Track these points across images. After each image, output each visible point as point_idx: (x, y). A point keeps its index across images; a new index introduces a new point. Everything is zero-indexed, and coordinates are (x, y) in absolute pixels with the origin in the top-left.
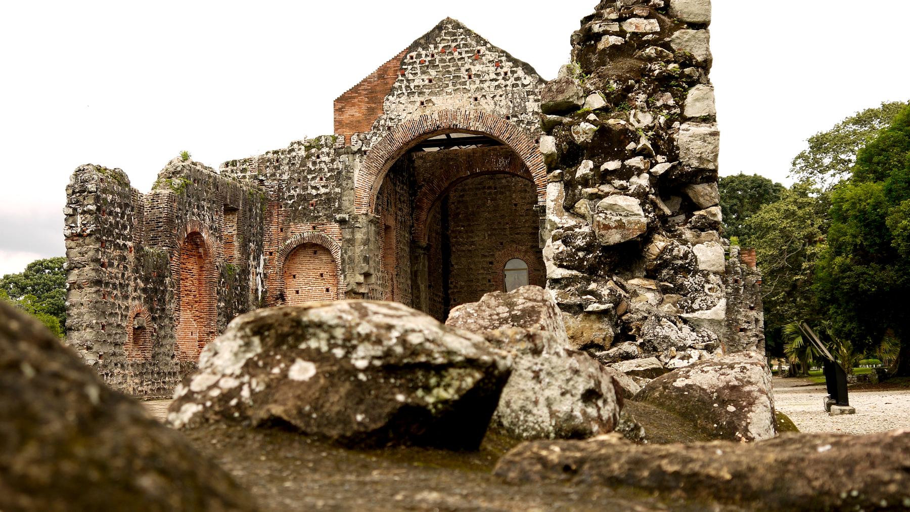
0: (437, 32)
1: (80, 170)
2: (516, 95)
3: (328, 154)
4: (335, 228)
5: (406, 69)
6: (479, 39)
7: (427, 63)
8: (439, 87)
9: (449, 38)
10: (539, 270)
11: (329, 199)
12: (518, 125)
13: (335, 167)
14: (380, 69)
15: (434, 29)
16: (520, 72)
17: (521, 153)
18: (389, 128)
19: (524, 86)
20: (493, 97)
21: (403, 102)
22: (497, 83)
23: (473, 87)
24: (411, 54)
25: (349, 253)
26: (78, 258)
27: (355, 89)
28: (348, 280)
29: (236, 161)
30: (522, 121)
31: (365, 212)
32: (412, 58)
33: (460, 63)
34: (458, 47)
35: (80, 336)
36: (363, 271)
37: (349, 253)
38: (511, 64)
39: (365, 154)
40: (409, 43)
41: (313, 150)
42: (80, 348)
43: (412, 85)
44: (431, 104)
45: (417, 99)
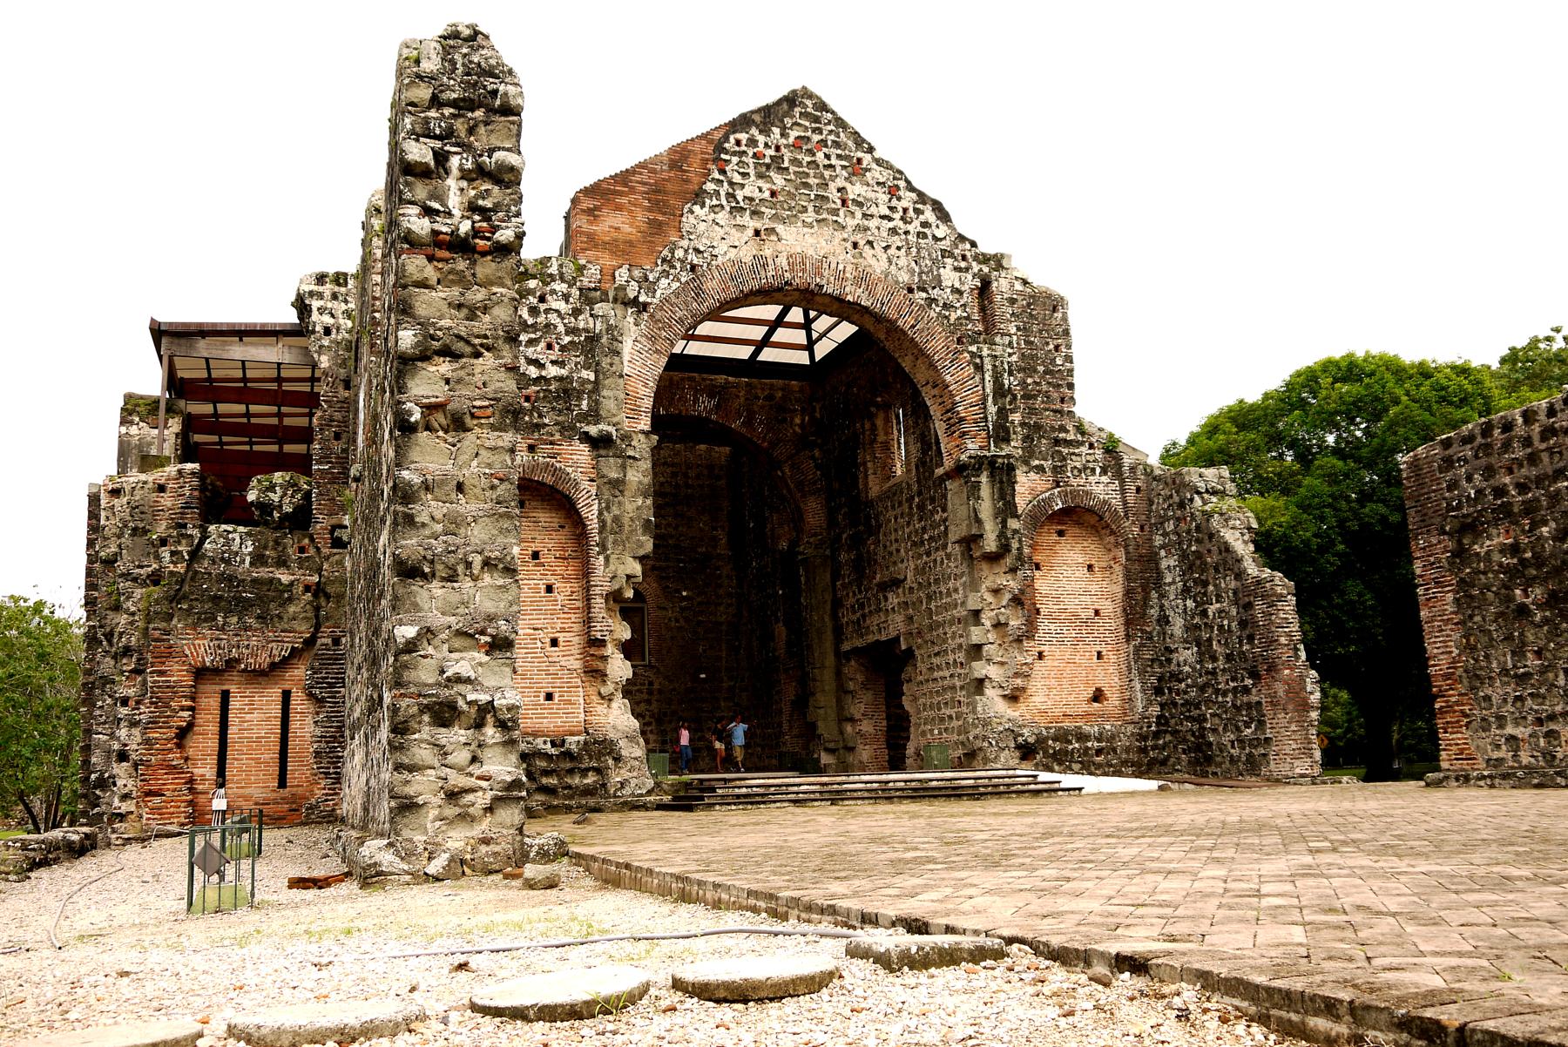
0: (785, 106)
1: (455, 35)
2: (924, 253)
3: (566, 297)
6: (859, 141)
7: (767, 160)
9: (807, 124)
10: (664, 609)
11: (566, 392)
12: (930, 306)
13: (582, 325)
14: (672, 150)
15: (779, 103)
16: (929, 215)
17: (936, 358)
18: (693, 268)
19: (936, 239)
20: (887, 248)
21: (722, 223)
22: (891, 225)
24: (739, 136)
25: (615, 511)
27: (623, 178)
28: (612, 567)
29: (345, 275)
31: (647, 428)
32: (738, 143)
33: (827, 174)
34: (823, 143)
35: (454, 598)
36: (641, 552)
37: (615, 511)
38: (914, 196)
39: (645, 310)
40: (733, 114)
41: (532, 284)
42: (458, 642)
43: (740, 195)
44: (774, 238)
45: (752, 224)
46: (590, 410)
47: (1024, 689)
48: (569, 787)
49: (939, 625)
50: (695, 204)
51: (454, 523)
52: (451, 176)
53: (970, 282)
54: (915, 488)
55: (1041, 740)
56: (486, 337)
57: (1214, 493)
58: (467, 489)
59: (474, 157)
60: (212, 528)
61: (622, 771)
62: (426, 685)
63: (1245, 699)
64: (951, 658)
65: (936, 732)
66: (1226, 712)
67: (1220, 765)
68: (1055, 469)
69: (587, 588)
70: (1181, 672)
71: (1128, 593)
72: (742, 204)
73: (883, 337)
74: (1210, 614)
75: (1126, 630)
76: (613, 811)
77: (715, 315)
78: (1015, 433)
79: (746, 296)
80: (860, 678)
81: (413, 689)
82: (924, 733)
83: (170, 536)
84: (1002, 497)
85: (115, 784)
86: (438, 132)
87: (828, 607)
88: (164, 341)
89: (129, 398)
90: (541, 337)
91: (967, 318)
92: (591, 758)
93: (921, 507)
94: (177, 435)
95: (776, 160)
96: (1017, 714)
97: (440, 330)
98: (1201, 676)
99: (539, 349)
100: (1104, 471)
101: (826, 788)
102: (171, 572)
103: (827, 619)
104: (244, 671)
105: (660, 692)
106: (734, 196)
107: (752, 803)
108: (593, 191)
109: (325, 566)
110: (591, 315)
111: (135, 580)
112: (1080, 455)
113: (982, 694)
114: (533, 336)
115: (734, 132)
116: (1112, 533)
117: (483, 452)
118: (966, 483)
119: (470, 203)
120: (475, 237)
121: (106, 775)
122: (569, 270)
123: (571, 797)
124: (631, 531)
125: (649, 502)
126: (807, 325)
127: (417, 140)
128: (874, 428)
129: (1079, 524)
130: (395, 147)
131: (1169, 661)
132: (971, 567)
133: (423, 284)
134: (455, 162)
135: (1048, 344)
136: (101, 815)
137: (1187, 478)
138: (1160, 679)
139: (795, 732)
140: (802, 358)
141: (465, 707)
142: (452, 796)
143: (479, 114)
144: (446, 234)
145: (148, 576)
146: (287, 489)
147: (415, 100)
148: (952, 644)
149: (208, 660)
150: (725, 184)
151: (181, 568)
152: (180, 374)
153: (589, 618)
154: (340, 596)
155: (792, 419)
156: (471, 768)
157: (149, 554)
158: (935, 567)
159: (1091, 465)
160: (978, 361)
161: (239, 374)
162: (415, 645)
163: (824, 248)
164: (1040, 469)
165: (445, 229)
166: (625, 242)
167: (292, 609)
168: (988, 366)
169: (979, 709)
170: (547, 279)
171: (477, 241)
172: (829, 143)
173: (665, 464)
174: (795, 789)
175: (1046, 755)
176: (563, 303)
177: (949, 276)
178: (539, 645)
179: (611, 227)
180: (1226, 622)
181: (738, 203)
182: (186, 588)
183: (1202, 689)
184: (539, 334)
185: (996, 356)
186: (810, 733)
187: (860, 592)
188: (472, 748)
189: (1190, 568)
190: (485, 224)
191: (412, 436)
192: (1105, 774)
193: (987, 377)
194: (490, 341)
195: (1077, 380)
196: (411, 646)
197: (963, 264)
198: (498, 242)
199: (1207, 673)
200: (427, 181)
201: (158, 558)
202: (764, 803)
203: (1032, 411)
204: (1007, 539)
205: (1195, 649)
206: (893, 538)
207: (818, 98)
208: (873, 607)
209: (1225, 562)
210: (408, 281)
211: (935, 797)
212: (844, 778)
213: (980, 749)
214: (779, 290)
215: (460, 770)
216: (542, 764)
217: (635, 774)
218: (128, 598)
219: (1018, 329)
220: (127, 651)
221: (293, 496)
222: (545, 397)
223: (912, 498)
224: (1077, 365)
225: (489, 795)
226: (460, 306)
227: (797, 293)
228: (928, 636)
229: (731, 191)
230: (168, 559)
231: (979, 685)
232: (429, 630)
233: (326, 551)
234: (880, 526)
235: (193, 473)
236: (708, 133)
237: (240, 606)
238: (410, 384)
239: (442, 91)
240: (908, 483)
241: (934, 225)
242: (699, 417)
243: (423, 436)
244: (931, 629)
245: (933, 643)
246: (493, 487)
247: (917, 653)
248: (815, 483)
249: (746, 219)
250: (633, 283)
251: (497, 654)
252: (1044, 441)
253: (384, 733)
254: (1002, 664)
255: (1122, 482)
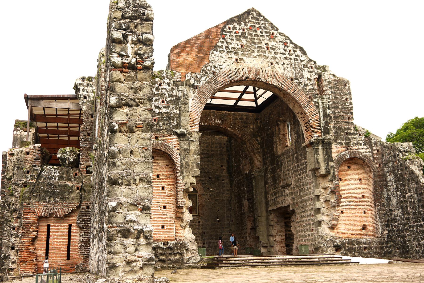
0: (246, 15)
2: (297, 66)
3: (169, 84)
4: (174, 139)
5: (226, 35)
6: (273, 26)
7: (240, 34)
8: (248, 51)
9: (254, 21)
10: (204, 195)
11: (169, 118)
12: (299, 85)
13: (174, 94)
14: (206, 31)
15: (244, 14)
16: (299, 52)
18: (214, 73)
20: (283, 64)
21: (224, 57)
22: (285, 56)
23: (270, 56)
26: (128, 94)
27: (189, 42)
28: (185, 180)
29: (92, 77)
30: (301, 83)
32: (229, 28)
33: (261, 38)
34: (260, 27)
35: (130, 192)
36: (196, 175)
37: (186, 160)
38: (293, 45)
39: (196, 88)
40: (228, 18)
41: (157, 79)
42: (131, 208)
43: (230, 47)
44: (242, 62)
46: (177, 124)
47: (336, 225)
48: (170, 260)
49: (304, 201)
50: (214, 50)
51: (130, 165)
52: (129, 43)
53: (314, 76)
54: (295, 151)
55: (343, 244)
56: (141, 99)
57: (407, 152)
58: (134, 153)
59: (136, 36)
60: (45, 167)
61: (189, 254)
62: (119, 223)
63: (421, 229)
64: (309, 213)
65: (304, 240)
66: (414, 234)
67: (412, 254)
68: (346, 144)
69: (176, 188)
70: (396, 219)
71: (375, 189)
72: (231, 50)
73: (282, 96)
74: (407, 197)
75: (375, 203)
76: (186, 269)
77: (222, 89)
78: (331, 130)
79: (233, 83)
80: (275, 220)
81: (115, 225)
82: (299, 241)
83: (30, 170)
84: (327, 154)
85: (10, 258)
86: (124, 28)
87: (263, 194)
88: (29, 101)
89: (17, 121)
90: (160, 98)
91: (313, 89)
92: (178, 249)
93: (297, 158)
94: (33, 134)
95: (243, 34)
96: (334, 234)
97: (125, 97)
98: (404, 220)
99: (159, 102)
100: (365, 144)
101: (263, 261)
102: (31, 183)
103: (263, 198)
104: (55, 217)
105: (202, 225)
106: (228, 47)
107: (236, 266)
108: (178, 46)
109: (84, 180)
110: (178, 90)
111: (18, 185)
112: (355, 138)
113: (320, 226)
114: (157, 98)
115: (228, 25)
116: (368, 167)
117: (140, 140)
118: (314, 149)
119: (135, 52)
120: (137, 64)
121: (7, 255)
122: (170, 74)
123: (170, 264)
124: (192, 167)
125: (198, 157)
126: (255, 93)
127: (117, 31)
128: (279, 129)
129: (356, 163)
130: (109, 33)
131: (391, 214)
132: (316, 179)
133: (119, 81)
134: (130, 38)
135: (343, 98)
136: (5, 269)
137: (396, 147)
138: (388, 221)
139: (252, 240)
140: (253, 104)
141: (133, 231)
142: (129, 263)
143: (138, 21)
144: (127, 63)
145: (23, 184)
146: (71, 153)
147: (116, 17)
148: (309, 208)
149: (43, 214)
150: (225, 43)
151: (34, 181)
152: (34, 113)
153: (177, 198)
154: (89, 191)
155: (250, 126)
156: (135, 253)
157: (23, 176)
158: (302, 180)
159: (360, 142)
160: (317, 104)
161: (55, 113)
162: (116, 209)
163: (261, 65)
164: (341, 144)
165: (126, 61)
166: (189, 64)
167: (72, 195)
168: (321, 106)
169: (320, 232)
170: (162, 78)
171: (138, 65)
172: (262, 27)
173: (204, 143)
174: (252, 261)
175: (345, 248)
176: (168, 86)
177: (306, 74)
178: (159, 208)
179: (184, 59)
180: (413, 200)
181: (229, 49)
182: (36, 188)
183: (404, 225)
184: (159, 97)
185: (324, 103)
186: (257, 240)
187: (275, 189)
188: (136, 245)
189: (399, 180)
190: (140, 60)
191: (115, 134)
192: (368, 257)
193: (321, 110)
194: (142, 101)
195: (354, 111)
196: (114, 209)
197: (311, 70)
198: (145, 66)
199: (406, 219)
200: (120, 45)
201: (26, 177)
202: (240, 266)
203: (338, 122)
204: (329, 169)
205: (401, 210)
206: (287, 169)
207: (258, 11)
208: (280, 194)
209: (412, 178)
210: (114, 80)
211: (304, 265)
212: (270, 257)
213: (320, 247)
214: (245, 80)
215: (131, 254)
216: (160, 251)
217: (194, 255)
218: (16, 192)
219: (332, 93)
220: (15, 211)
221: (73, 156)
222: (161, 120)
223: (294, 154)
224: (354, 106)
225: (142, 263)
226: (132, 88)
227: (251, 81)
228: (300, 205)
229: (227, 45)
230: (29, 178)
231: (320, 223)
232: (120, 203)
233: (84, 175)
234: (282, 165)
235: (39, 148)
236: (219, 25)
237: (54, 194)
238: (114, 116)
239: (125, 14)
240: (292, 149)
241: (300, 56)
242: (216, 126)
243: (119, 134)
244: (301, 202)
245: (302, 207)
246: (143, 152)
247: (296, 211)
248: (258, 149)
249: (232, 55)
250: (192, 79)
251: (145, 212)
252: (342, 133)
253: (104, 240)
254: (328, 215)
255: (372, 148)
